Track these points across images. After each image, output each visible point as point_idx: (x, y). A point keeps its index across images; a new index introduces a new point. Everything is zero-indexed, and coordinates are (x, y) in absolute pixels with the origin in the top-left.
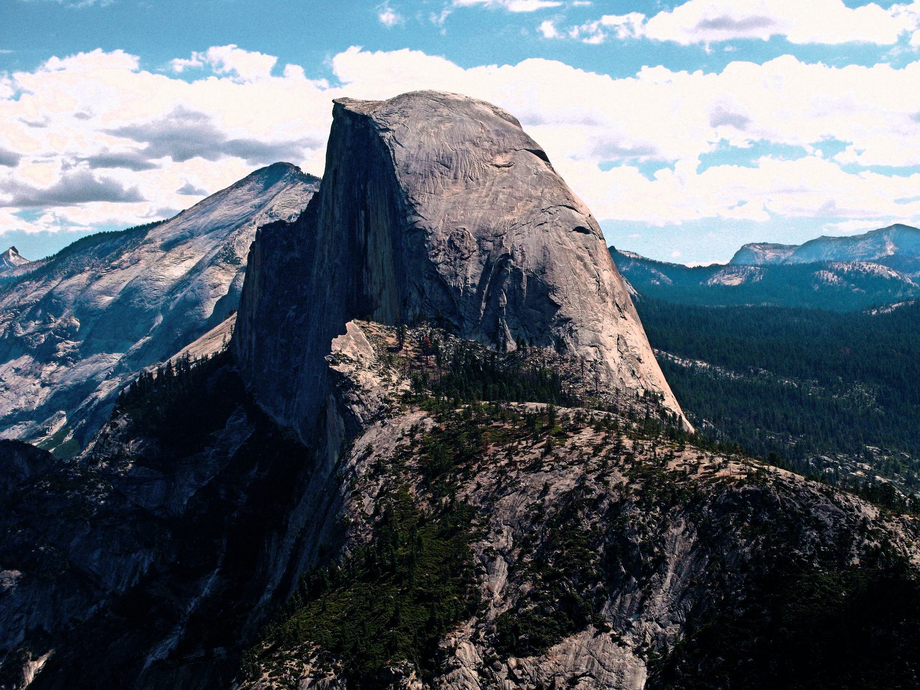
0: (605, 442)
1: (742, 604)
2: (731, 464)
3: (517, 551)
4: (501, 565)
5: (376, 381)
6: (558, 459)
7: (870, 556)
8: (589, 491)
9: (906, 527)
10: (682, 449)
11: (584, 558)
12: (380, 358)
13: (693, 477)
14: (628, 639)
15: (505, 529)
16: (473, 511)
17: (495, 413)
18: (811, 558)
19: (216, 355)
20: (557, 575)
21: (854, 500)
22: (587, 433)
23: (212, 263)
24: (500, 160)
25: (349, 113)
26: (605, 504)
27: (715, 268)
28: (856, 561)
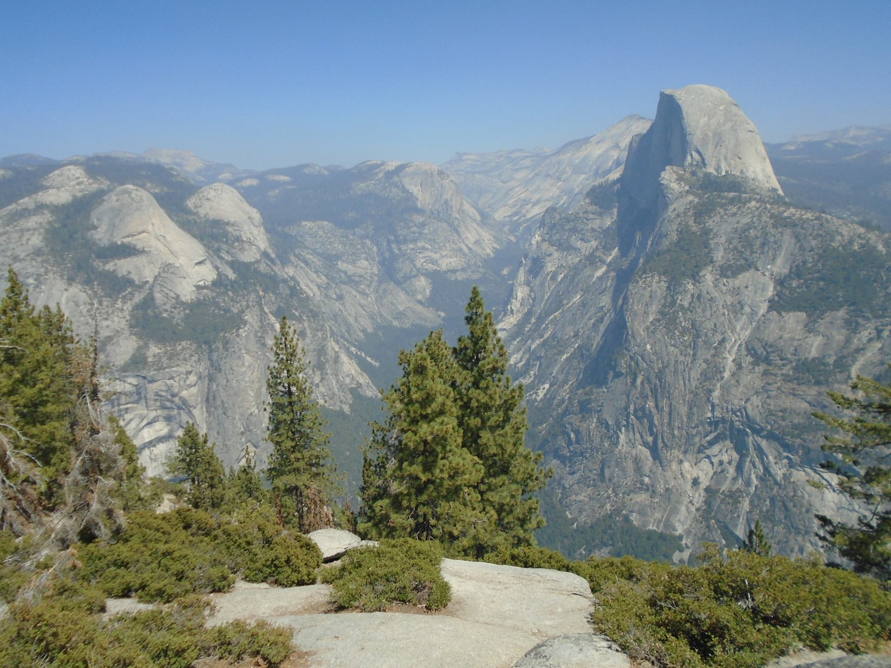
0: (760, 206)
1: (810, 263)
2: (808, 214)
3: (727, 243)
4: (721, 248)
5: (677, 186)
6: (742, 212)
7: (862, 246)
8: (754, 223)
9: (876, 237)
10: (789, 208)
11: (751, 246)
12: (677, 179)
13: (794, 218)
14: (767, 274)
15: (723, 236)
16: (711, 230)
17: (719, 196)
18: (838, 247)
19: (618, 179)
20: (743, 252)
21: (856, 226)
22: (753, 203)
23: (612, 148)
24: (722, 108)
25: (666, 95)
26: (760, 227)
27: (784, 145)
28: (856, 248)
